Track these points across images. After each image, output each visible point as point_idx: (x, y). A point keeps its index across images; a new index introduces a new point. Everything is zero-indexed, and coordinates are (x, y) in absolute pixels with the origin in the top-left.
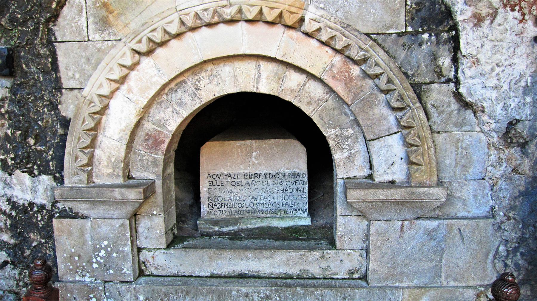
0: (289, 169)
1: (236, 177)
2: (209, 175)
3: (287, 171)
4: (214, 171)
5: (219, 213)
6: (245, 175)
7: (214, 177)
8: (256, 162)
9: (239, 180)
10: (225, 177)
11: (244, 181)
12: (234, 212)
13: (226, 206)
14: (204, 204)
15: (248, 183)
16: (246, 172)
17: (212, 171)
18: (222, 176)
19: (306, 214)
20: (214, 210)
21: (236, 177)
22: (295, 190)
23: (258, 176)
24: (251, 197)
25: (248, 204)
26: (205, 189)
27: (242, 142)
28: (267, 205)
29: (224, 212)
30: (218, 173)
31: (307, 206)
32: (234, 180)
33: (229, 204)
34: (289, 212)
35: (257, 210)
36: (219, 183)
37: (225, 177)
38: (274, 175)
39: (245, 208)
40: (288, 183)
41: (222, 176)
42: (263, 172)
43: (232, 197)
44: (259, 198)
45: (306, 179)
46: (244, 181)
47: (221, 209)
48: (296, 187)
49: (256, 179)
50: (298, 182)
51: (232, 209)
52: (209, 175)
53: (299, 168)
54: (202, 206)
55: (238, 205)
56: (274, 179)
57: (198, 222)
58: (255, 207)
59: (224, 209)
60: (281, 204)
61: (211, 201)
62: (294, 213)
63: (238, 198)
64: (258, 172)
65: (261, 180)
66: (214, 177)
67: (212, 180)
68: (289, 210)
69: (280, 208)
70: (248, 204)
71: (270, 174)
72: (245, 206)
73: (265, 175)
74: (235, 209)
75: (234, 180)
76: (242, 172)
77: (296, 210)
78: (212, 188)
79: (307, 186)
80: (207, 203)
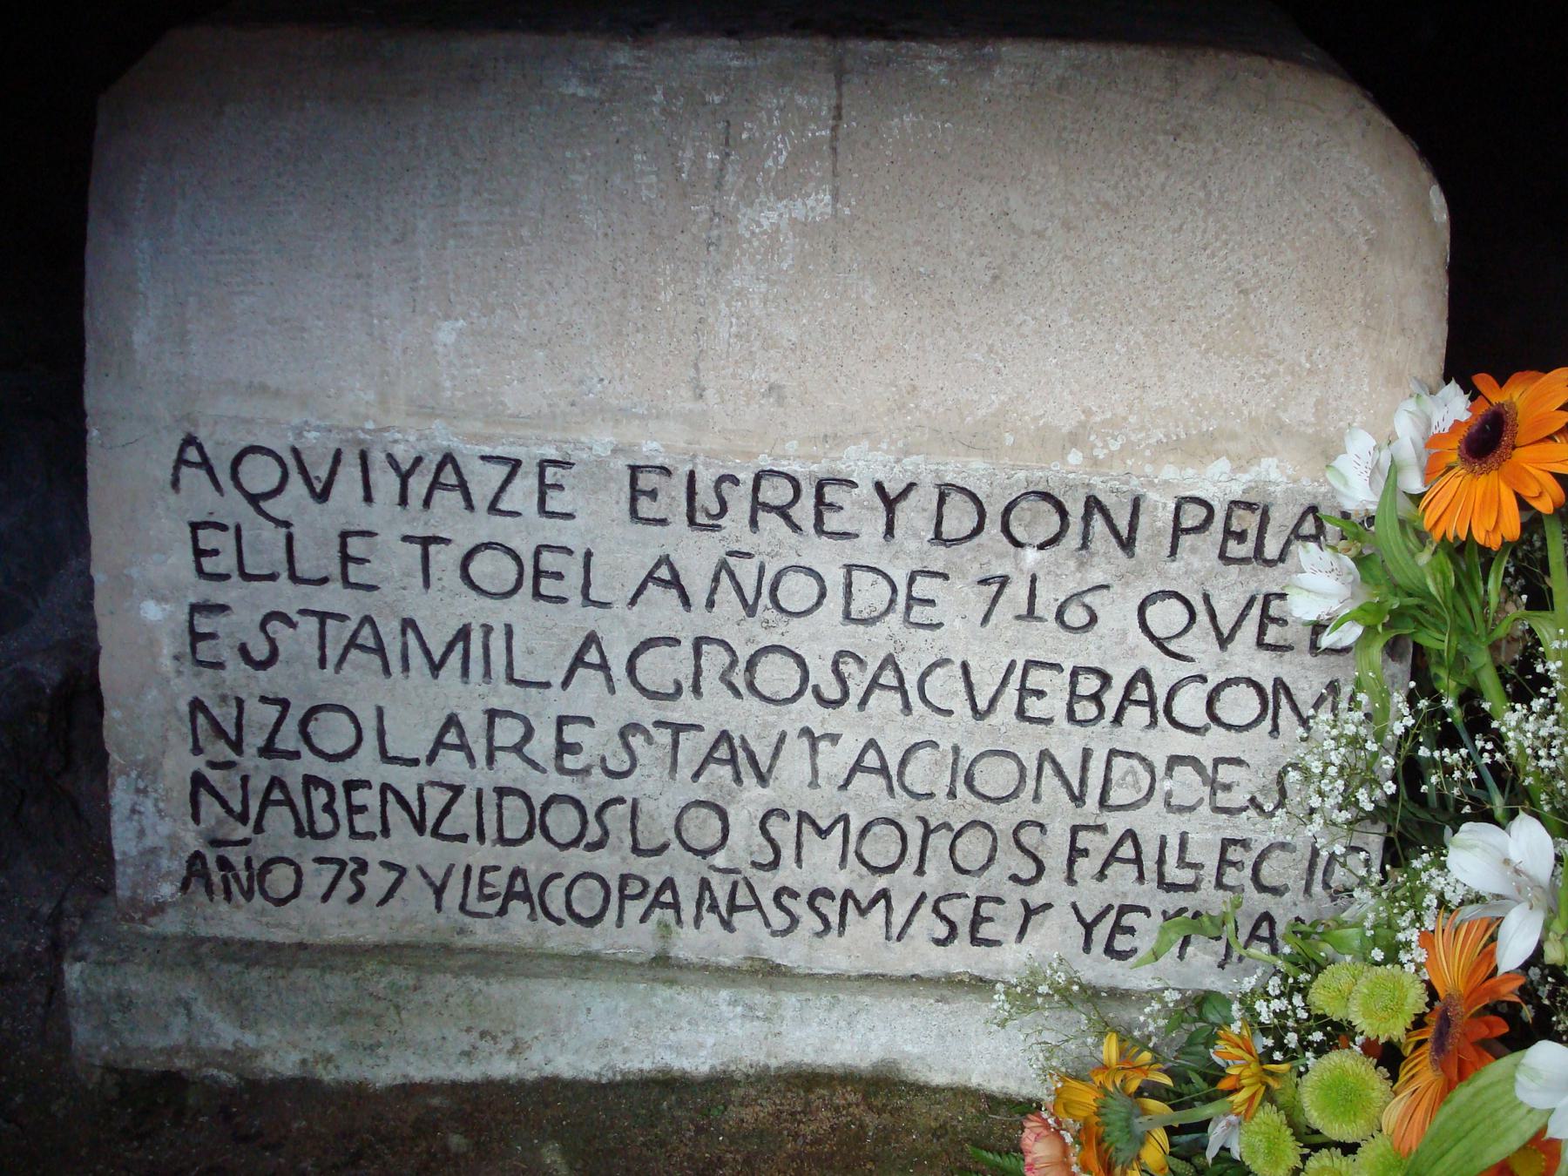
0: (1200, 448)
1: (521, 495)
3: (1169, 472)
6: (639, 484)
7: (259, 475)
9: (552, 532)
10: (384, 483)
11: (625, 553)
12: (499, 881)
14: (149, 770)
16: (651, 449)
18: (350, 473)
20: (263, 849)
21: (521, 495)
22: (1240, 705)
23: (804, 512)
24: (693, 747)
26: (152, 611)
28: (881, 848)
29: (378, 881)
33: (436, 799)
36: (316, 557)
37: (384, 483)
41: (350, 473)
42: (866, 463)
43: (474, 724)
44: (795, 757)
47: (342, 846)
48: (1264, 668)
52: (191, 453)
54: (121, 796)
56: (991, 554)
57: (73, 973)
59: (372, 851)
61: (224, 752)
63: (543, 745)
65: (827, 558)
66: (259, 475)
67: (233, 507)
69: (1036, 896)
74: (510, 858)
78: (246, 605)
80: (180, 764)
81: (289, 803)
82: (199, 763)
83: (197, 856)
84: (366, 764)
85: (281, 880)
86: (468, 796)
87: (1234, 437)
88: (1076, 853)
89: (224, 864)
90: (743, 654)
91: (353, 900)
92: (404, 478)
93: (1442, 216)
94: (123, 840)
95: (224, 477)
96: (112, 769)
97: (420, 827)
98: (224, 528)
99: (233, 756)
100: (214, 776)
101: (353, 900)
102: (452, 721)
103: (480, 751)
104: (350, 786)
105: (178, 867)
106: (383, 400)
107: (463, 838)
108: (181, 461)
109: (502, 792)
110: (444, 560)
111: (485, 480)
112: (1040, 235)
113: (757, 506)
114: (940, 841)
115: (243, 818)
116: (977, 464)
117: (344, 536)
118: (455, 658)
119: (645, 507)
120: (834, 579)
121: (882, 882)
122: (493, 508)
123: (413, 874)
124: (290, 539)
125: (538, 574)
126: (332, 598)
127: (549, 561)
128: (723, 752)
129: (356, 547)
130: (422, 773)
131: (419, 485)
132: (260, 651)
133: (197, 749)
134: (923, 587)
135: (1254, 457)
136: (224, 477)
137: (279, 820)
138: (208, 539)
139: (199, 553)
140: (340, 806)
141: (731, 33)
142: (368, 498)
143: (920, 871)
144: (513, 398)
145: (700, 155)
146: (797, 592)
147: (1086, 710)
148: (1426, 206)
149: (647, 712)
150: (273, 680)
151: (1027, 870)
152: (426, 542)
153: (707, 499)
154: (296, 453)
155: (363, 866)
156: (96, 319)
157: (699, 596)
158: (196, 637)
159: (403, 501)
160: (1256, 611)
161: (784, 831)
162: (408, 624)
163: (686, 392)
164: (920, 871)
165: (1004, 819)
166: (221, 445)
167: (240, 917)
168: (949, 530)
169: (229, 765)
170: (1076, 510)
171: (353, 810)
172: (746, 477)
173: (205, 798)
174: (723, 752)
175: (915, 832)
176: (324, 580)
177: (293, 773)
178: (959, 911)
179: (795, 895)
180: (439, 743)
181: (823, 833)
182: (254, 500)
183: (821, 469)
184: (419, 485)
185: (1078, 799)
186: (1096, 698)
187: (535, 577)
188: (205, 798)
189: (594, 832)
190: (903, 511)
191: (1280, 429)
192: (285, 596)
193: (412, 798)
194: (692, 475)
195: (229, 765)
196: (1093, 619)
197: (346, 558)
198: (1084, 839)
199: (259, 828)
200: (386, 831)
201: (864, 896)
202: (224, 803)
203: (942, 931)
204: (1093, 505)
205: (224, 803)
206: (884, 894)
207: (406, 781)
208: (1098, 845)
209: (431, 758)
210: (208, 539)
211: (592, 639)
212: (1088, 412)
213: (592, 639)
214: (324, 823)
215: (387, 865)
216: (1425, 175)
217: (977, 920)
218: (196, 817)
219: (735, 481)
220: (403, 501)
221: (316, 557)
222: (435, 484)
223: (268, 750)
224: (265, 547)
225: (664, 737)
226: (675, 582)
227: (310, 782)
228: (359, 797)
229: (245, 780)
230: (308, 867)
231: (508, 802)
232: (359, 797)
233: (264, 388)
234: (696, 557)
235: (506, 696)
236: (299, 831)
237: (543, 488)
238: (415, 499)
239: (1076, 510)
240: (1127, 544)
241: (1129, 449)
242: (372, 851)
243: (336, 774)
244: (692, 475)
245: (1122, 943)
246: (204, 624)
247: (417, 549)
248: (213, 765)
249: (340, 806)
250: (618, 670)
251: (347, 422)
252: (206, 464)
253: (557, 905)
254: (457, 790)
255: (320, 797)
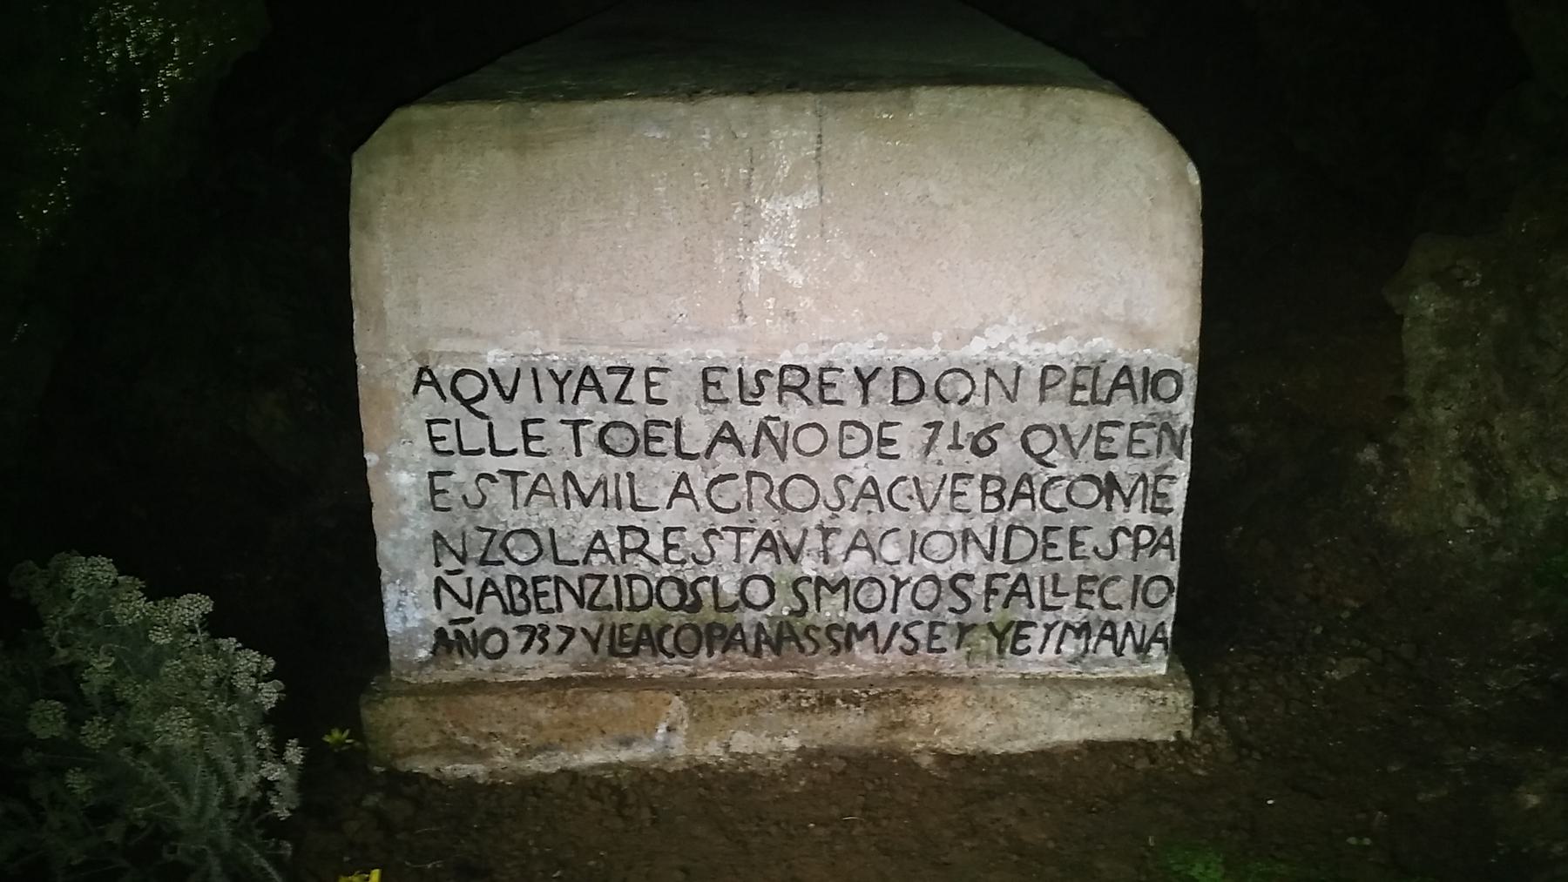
0: (1055, 334)
1: (636, 390)
2: (424, 376)
4: (460, 345)
5: (517, 642)
6: (707, 378)
7: (470, 387)
8: (796, 278)
9: (656, 412)
10: (549, 388)
12: (631, 634)
13: (568, 601)
14: (409, 575)
15: (726, 435)
16: (715, 352)
17: (444, 345)
18: (526, 383)
19: (1158, 665)
21: (636, 390)
23: (811, 390)
24: (749, 541)
25: (729, 587)
27: (681, 109)
29: (556, 638)
30: (495, 358)
31: (1172, 606)
32: (623, 412)
33: (591, 585)
34: (1036, 644)
35: (798, 624)
36: (509, 438)
38: (930, 380)
39: (708, 614)
40: (1040, 442)
41: (526, 383)
45: (1184, 411)
46: (699, 430)
47: (534, 619)
48: (1100, 469)
49: (796, 412)
50: (1120, 435)
51: (620, 617)
52: (424, 376)
53: (1134, 332)
54: (390, 596)
55: (655, 594)
58: (784, 606)
59: (553, 621)
60: (980, 586)
61: (451, 563)
62: (1069, 649)
63: (656, 547)
64: (813, 363)
65: (831, 417)
67: (454, 409)
68: (1037, 634)
69: (968, 618)
70: (729, 587)
71: (898, 371)
72: (708, 601)
73: (864, 380)
74: (638, 618)
75: (623, 412)
76: (684, 355)
77: (1084, 630)
79: (1182, 469)
81: (497, 593)
82: (440, 572)
83: (441, 633)
84: (545, 567)
85: (494, 643)
86: (610, 581)
87: (1076, 326)
88: (990, 591)
89: (458, 633)
90: (777, 482)
91: (541, 651)
92: (561, 384)
93: (1196, 181)
94: (393, 624)
95: (447, 392)
96: (384, 579)
97: (580, 602)
98: (448, 422)
99: (460, 566)
100: (449, 580)
101: (541, 651)
102: (599, 535)
103: (616, 553)
104: (536, 580)
105: (431, 639)
106: (545, 336)
107: (610, 607)
108: (420, 382)
109: (630, 578)
110: (588, 434)
111: (612, 383)
112: (949, 207)
113: (783, 388)
114: (905, 592)
115: (469, 605)
116: (918, 352)
117: (525, 423)
118: (599, 496)
119: (713, 392)
120: (833, 434)
121: (872, 617)
122: (618, 399)
123: (579, 634)
124: (490, 426)
125: (648, 439)
126: (517, 462)
127: (655, 431)
128: (768, 543)
129: (533, 430)
130: (580, 570)
131: (570, 388)
132: (475, 498)
133: (438, 564)
134: (888, 433)
135: (1089, 338)
136: (447, 392)
137: (492, 602)
138: (438, 430)
139: (433, 439)
140: (530, 592)
141: (751, 93)
142: (539, 399)
143: (894, 610)
144: (630, 329)
145: (735, 170)
146: (810, 440)
147: (993, 503)
148: (1184, 176)
149: (722, 520)
150: (483, 517)
151: (961, 606)
152: (576, 424)
153: (752, 385)
154: (491, 371)
155: (547, 630)
156: (359, 292)
157: (749, 448)
158: (434, 492)
159: (562, 400)
160: (1094, 434)
161: (807, 590)
162: (569, 476)
163: (735, 320)
164: (894, 610)
165: (944, 574)
166: (444, 371)
167: (470, 667)
168: (901, 396)
169: (458, 572)
170: (980, 378)
171: (537, 595)
172: (775, 370)
173: (444, 592)
174: (768, 543)
175: (890, 585)
176: (514, 452)
177: (499, 575)
178: (919, 633)
179: (818, 629)
180: (591, 550)
181: (834, 590)
182: (467, 403)
183: (820, 360)
184: (570, 388)
185: (990, 557)
186: (998, 494)
187: (644, 442)
188: (444, 592)
189: (691, 598)
190: (872, 385)
191: (1104, 320)
192: (490, 463)
193: (575, 585)
194: (740, 371)
195: (458, 572)
196: (994, 445)
197: (527, 438)
198: (998, 583)
199: (479, 611)
200: (560, 608)
201: (861, 626)
202: (456, 596)
203: (910, 645)
204: (991, 373)
205: (456, 596)
206: (872, 627)
207: (572, 575)
208: (1003, 586)
209: (586, 561)
210: (438, 430)
211: (684, 477)
212: (985, 317)
213: (684, 477)
214: (520, 604)
215: (561, 628)
216: (1184, 156)
217: (932, 637)
218: (439, 606)
219: (767, 373)
220: (562, 400)
221: (509, 438)
222: (581, 387)
223: (483, 562)
224: (475, 435)
225: (731, 536)
226: (734, 440)
227: (510, 579)
228: (541, 587)
229: (469, 580)
230: (511, 633)
231: (635, 583)
232: (541, 587)
233: (469, 332)
234: (746, 421)
235: (634, 519)
236: (505, 611)
237: (649, 384)
238: (568, 397)
239: (980, 378)
240: (1011, 397)
241: (1013, 339)
242: (553, 621)
243: (527, 574)
244: (740, 371)
245: (1020, 646)
246: (440, 483)
247: (569, 428)
248: (449, 573)
249: (530, 592)
250: (699, 496)
251: (523, 351)
252: (434, 383)
253: (668, 642)
254: (603, 578)
255: (517, 588)
